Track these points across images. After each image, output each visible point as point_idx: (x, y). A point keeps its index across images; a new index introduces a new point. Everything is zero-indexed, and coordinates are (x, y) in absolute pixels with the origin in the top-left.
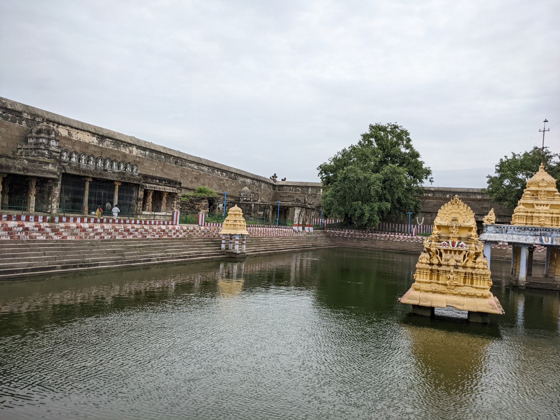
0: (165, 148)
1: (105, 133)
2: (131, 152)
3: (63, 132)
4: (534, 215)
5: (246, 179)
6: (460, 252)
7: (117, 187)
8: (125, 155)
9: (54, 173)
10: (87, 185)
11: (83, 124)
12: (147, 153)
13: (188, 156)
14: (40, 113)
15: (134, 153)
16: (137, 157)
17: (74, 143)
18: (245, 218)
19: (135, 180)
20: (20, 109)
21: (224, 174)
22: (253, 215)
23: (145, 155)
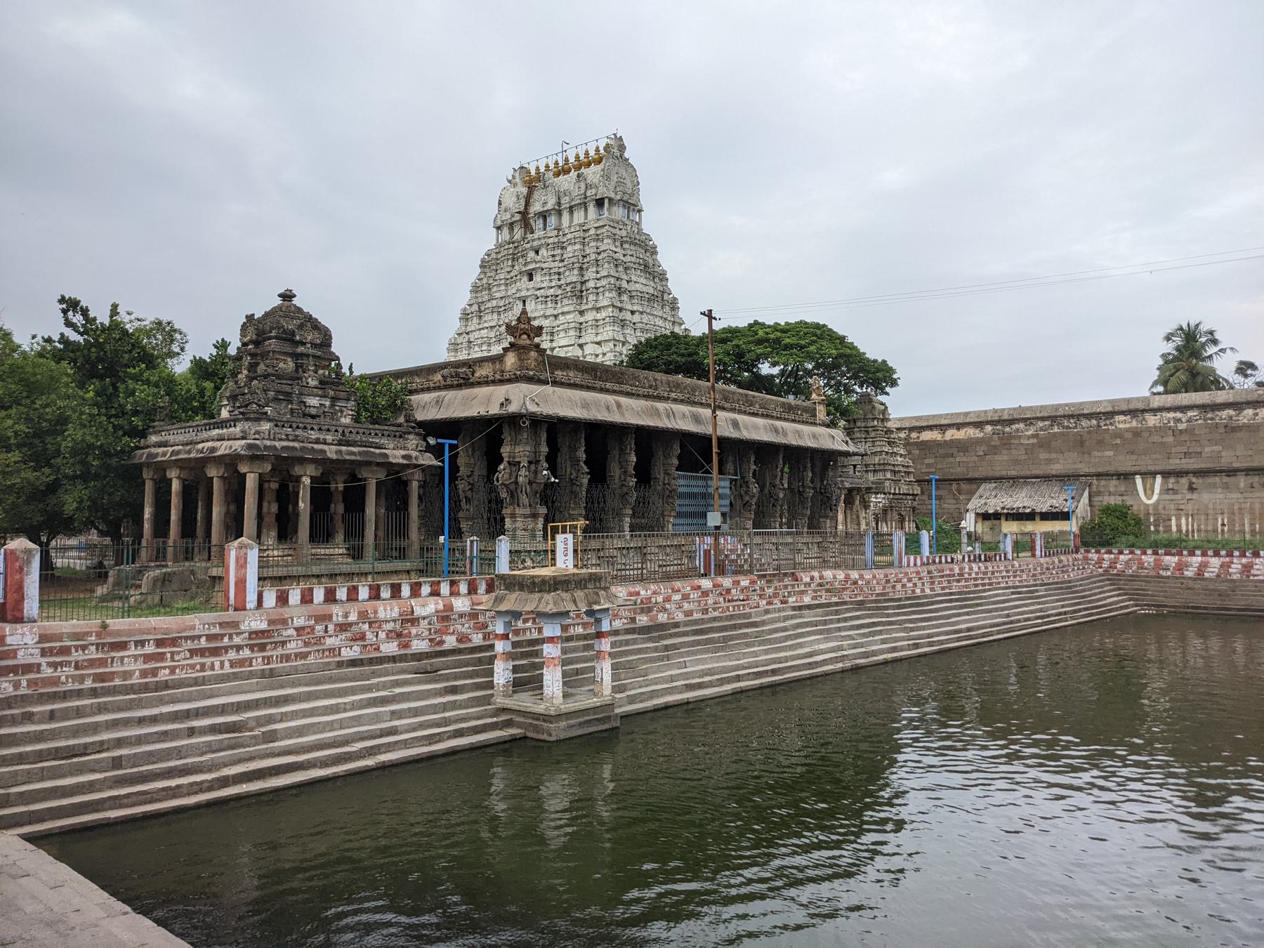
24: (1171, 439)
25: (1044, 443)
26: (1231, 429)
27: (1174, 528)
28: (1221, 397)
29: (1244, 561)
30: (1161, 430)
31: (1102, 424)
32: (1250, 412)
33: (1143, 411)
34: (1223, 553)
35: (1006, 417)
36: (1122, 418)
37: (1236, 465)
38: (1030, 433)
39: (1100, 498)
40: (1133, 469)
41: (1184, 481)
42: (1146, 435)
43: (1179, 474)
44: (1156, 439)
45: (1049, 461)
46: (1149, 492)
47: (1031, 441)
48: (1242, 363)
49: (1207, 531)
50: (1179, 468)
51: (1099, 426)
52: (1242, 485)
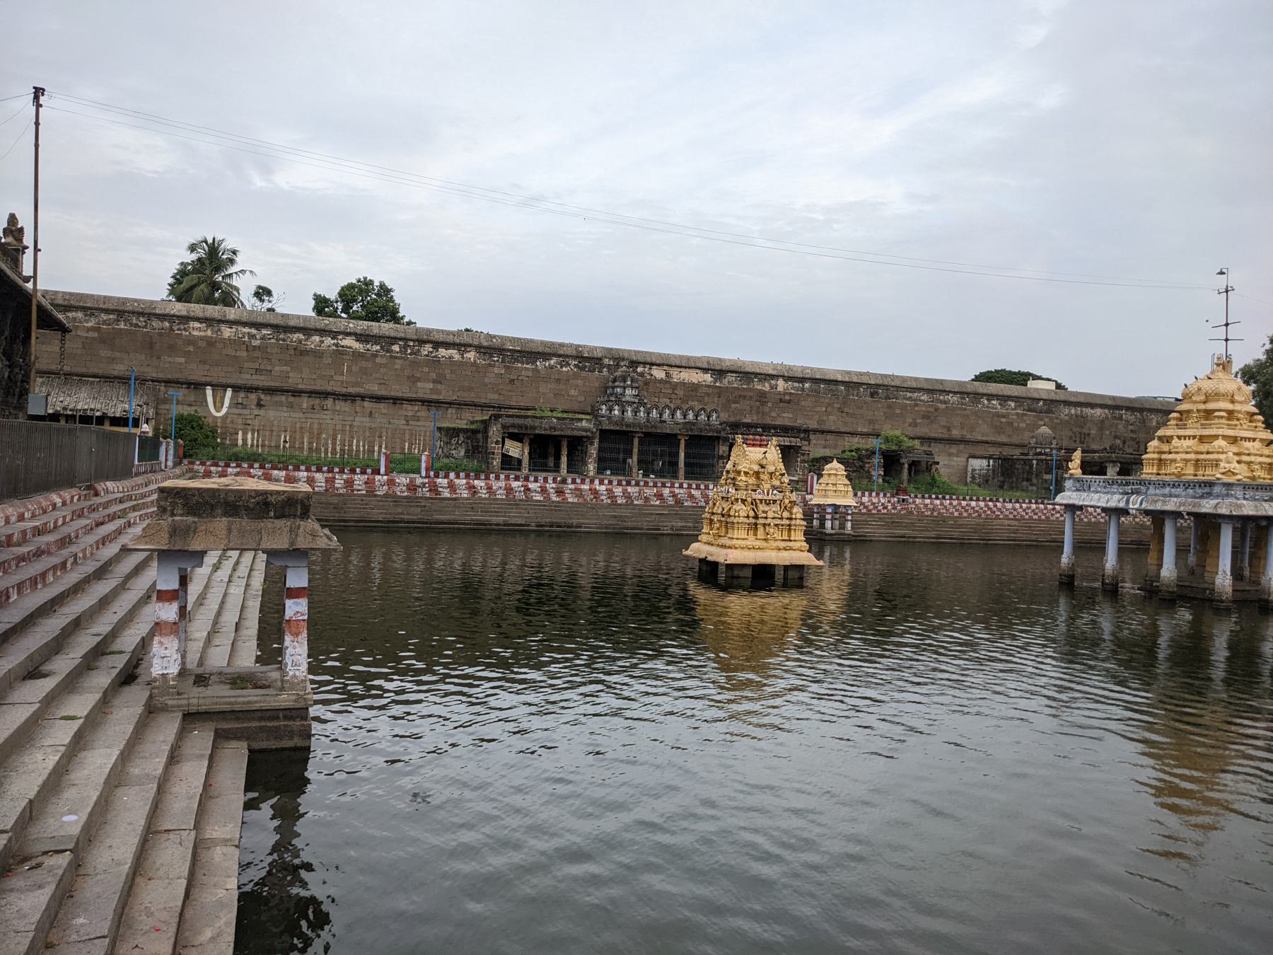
0: (849, 373)
1: (724, 366)
2: (774, 387)
3: (659, 374)
4: (1164, 456)
5: (1089, 411)
6: (775, 501)
7: (683, 442)
8: (762, 395)
9: (586, 430)
10: (636, 441)
11: (689, 358)
12: (807, 385)
13: (904, 379)
14: (626, 355)
15: (780, 389)
16: (785, 394)
17: (675, 386)
18: (850, 480)
19: (711, 430)
20: (600, 355)
21: (1013, 404)
22: (1035, 481)
23: (803, 389)
24: (245, 354)
25: (108, 339)
26: (301, 352)
27: (240, 442)
28: (232, 313)
29: (345, 476)
30: (236, 343)
31: (175, 328)
32: (317, 338)
33: (220, 321)
34: (325, 469)
35: (60, 302)
36: (197, 325)
37: (300, 387)
38: (90, 324)
39: (167, 407)
40: (204, 379)
41: (253, 396)
42: (220, 346)
43: (250, 389)
44: (231, 352)
45: (112, 360)
46: (218, 405)
47: (91, 334)
48: (260, 287)
49: (270, 446)
50: (249, 383)
51: (171, 329)
52: (305, 406)
